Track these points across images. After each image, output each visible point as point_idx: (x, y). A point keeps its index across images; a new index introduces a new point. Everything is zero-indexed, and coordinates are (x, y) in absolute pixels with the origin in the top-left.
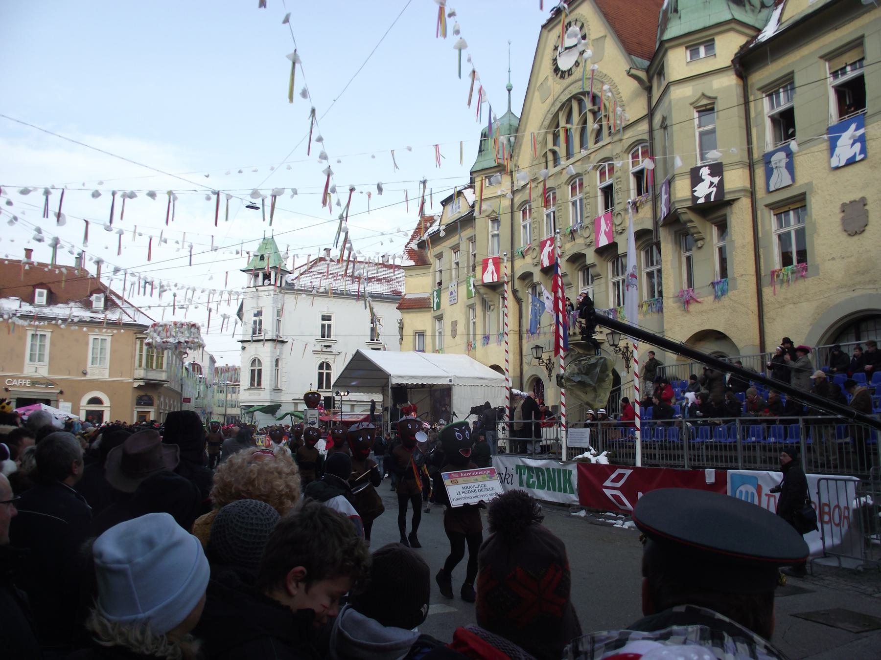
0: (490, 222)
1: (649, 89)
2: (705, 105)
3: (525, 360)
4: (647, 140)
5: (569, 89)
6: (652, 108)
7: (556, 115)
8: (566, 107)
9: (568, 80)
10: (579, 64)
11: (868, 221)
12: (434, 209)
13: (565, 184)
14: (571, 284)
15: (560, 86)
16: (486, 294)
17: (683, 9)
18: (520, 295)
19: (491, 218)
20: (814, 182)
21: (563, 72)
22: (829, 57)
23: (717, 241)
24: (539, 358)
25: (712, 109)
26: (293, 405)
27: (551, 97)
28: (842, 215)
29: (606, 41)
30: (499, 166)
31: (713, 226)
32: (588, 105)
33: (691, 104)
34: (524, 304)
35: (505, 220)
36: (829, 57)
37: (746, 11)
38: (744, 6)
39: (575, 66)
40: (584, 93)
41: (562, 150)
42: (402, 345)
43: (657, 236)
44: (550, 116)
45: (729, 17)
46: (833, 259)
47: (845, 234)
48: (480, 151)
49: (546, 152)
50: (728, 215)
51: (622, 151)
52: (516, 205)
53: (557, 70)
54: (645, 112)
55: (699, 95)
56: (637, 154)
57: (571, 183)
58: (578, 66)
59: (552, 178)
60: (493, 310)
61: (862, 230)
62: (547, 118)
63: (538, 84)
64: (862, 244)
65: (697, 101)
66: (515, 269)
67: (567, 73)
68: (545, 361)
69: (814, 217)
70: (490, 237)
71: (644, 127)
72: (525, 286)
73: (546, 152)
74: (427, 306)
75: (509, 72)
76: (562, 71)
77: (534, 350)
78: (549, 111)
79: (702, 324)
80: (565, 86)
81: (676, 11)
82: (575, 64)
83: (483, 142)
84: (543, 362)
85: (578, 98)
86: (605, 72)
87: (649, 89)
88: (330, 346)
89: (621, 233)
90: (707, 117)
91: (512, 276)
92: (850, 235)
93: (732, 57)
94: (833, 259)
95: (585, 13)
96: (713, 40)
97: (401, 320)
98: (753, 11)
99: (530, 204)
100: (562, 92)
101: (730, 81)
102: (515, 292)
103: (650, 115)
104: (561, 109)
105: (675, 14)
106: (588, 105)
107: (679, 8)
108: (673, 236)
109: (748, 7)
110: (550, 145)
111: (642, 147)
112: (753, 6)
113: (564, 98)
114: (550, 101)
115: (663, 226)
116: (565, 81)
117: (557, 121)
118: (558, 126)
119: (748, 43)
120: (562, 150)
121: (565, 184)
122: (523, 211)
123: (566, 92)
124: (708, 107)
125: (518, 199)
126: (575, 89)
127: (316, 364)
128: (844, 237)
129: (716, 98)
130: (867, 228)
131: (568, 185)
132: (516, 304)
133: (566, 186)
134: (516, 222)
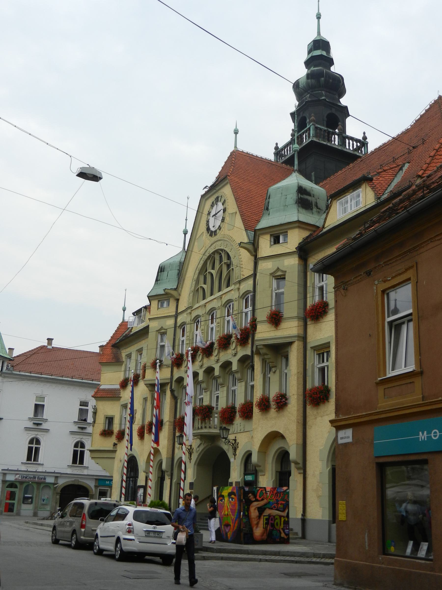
2: (280, 276)
5: (214, 245)
7: (205, 263)
8: (211, 257)
9: (214, 239)
10: (221, 228)
12: (129, 317)
15: (209, 241)
17: (272, 208)
18: (176, 393)
19: (160, 333)
21: (212, 232)
25: (284, 278)
26: (2, 475)
27: (204, 248)
30: (166, 294)
32: (225, 260)
33: (271, 274)
37: (313, 213)
38: (312, 209)
39: (218, 229)
40: (222, 250)
42: (94, 428)
43: (252, 361)
44: (202, 262)
45: (296, 219)
48: (157, 280)
50: (289, 352)
52: (178, 325)
53: (208, 229)
55: (276, 268)
57: (211, 314)
59: (200, 308)
62: (200, 263)
65: (275, 272)
70: (159, 347)
74: (117, 396)
75: (186, 220)
76: (211, 231)
78: (202, 258)
80: (212, 242)
81: (267, 209)
83: (160, 273)
85: (218, 252)
88: (41, 424)
90: (282, 282)
93: (297, 245)
96: (287, 232)
97: (95, 406)
98: (319, 212)
100: (210, 247)
102: (172, 391)
105: (266, 211)
106: (225, 260)
107: (269, 208)
108: (261, 362)
109: (315, 209)
112: (320, 209)
113: (211, 250)
114: (203, 251)
115: (256, 354)
119: (311, 235)
123: (212, 247)
124: (282, 277)
127: (28, 438)
129: (286, 272)
131: (209, 315)
132: (173, 400)
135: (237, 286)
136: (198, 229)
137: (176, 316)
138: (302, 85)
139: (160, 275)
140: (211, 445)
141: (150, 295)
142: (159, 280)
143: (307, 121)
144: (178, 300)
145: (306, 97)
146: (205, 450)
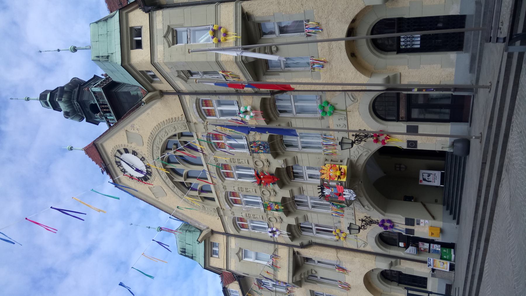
0: (246, 259)
1: (162, 93)
3: (362, 248)
4: (197, 100)
6: (175, 92)
9: (153, 169)
10: (143, 157)
13: (223, 182)
14: (300, 188)
16: (301, 274)
18: (305, 242)
23: (275, 35)
24: (359, 229)
29: (129, 131)
31: (262, 38)
34: (314, 240)
35: (245, 244)
41: (201, 184)
49: (200, 196)
52: (237, 233)
54: (176, 97)
56: (207, 111)
58: (144, 158)
60: (316, 272)
63: (154, 197)
67: (148, 169)
68: (363, 224)
71: (187, 99)
72: (300, 236)
73: (200, 196)
77: (352, 231)
82: (142, 161)
83: (186, 254)
84: (363, 226)
86: (149, 134)
87: (162, 93)
95: (111, 149)
99: (236, 220)
101: (159, 15)
102: (302, 246)
103: (179, 93)
104: (172, 179)
110: (196, 193)
111: (203, 106)
116: (153, 172)
117: (180, 184)
118: (182, 183)
120: (201, 184)
121: (223, 182)
122: (241, 228)
125: (231, 230)
126: (159, 164)
131: (225, 179)
133: (226, 182)
134: (248, 235)
135: (192, 124)
136: (147, 196)
137: (227, 234)
138: (67, 108)
139: (188, 253)
140: (361, 182)
141: (203, 266)
142: (192, 255)
143: (93, 103)
144: (213, 232)
145: (76, 105)
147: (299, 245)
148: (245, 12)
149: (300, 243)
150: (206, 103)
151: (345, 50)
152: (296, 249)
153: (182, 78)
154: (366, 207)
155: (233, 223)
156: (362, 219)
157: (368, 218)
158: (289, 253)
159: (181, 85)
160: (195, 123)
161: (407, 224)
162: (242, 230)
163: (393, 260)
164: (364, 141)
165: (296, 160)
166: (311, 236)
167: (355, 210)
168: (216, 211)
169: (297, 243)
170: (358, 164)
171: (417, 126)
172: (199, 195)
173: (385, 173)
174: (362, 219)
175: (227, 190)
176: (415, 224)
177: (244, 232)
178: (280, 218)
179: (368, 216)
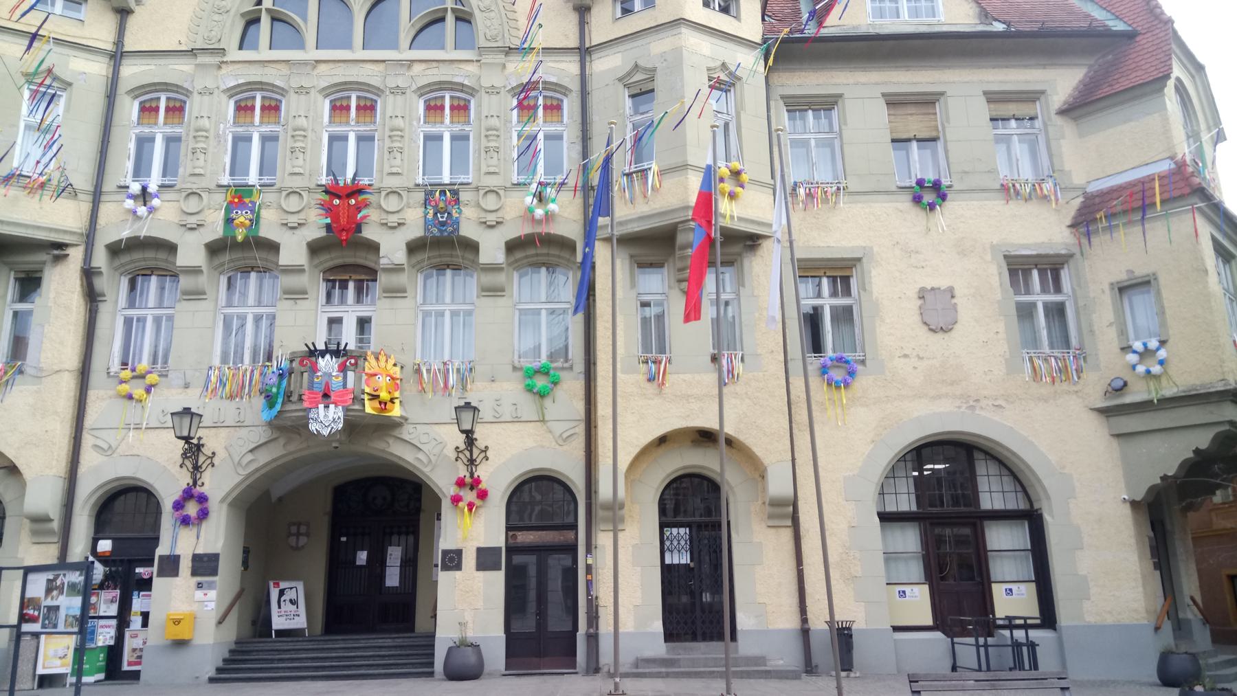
3: (88, 440)
11: (957, 318)
14: (306, 293)
18: (101, 284)
20: (875, 249)
22: (895, 102)
28: (920, 302)
34: (105, 310)
36: (895, 102)
46: (906, 356)
47: (926, 328)
51: (505, 87)
52: (123, 87)
57: (333, 97)
61: (950, 327)
64: (948, 345)
66: (102, 220)
69: (875, 294)
72: (116, 269)
79: (688, 416)
89: (491, 227)
91: (89, 237)
92: (931, 330)
94: (906, 356)
102: (89, 274)
125: (133, 72)
128: (922, 331)
130: (955, 326)
135: (500, 58)
137: (117, 56)
146: (279, 463)
147: (95, 264)
148: (760, 241)
149: (100, 268)
150: (554, 108)
151: (685, 426)
152: (76, 255)
153: (629, 74)
154: (250, 457)
155: (166, 84)
156: (203, 445)
157: (209, 461)
158: (65, 232)
159: (606, 65)
160: (504, 66)
161: (196, 558)
162: (132, 105)
163: (55, 525)
164: (458, 457)
165: (394, 295)
166: (117, 301)
167: (237, 429)
168: (208, 42)
169: (100, 259)
170: (391, 441)
171: (500, 569)
172: (266, 9)
173: (280, 499)
174: (203, 445)
175: (293, 97)
176: (199, 579)
177: (129, 109)
178: (198, 225)
179: (216, 461)
